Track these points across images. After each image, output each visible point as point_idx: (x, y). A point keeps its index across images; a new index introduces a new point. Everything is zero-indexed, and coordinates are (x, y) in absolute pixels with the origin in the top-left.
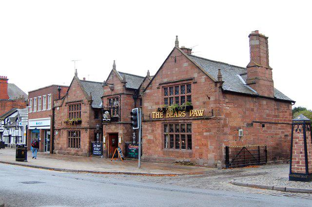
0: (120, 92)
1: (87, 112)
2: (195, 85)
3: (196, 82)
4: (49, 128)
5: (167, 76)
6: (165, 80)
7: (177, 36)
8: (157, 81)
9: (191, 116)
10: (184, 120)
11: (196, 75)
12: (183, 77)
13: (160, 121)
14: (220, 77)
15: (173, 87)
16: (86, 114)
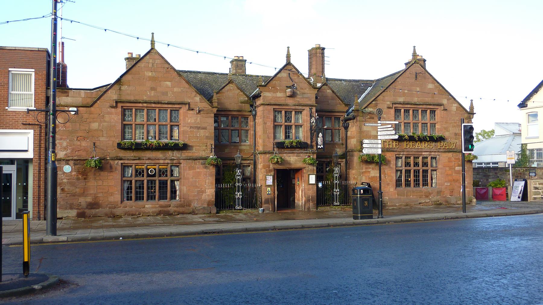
0: (309, 103)
1: (205, 128)
2: (445, 112)
3: (446, 110)
4: (30, 155)
5: (404, 95)
6: (401, 100)
7: (414, 47)
8: (386, 98)
9: (439, 147)
10: (430, 152)
11: (445, 102)
12: (428, 100)
13: (394, 151)
14: (472, 108)
15: (409, 110)
16: (202, 131)
